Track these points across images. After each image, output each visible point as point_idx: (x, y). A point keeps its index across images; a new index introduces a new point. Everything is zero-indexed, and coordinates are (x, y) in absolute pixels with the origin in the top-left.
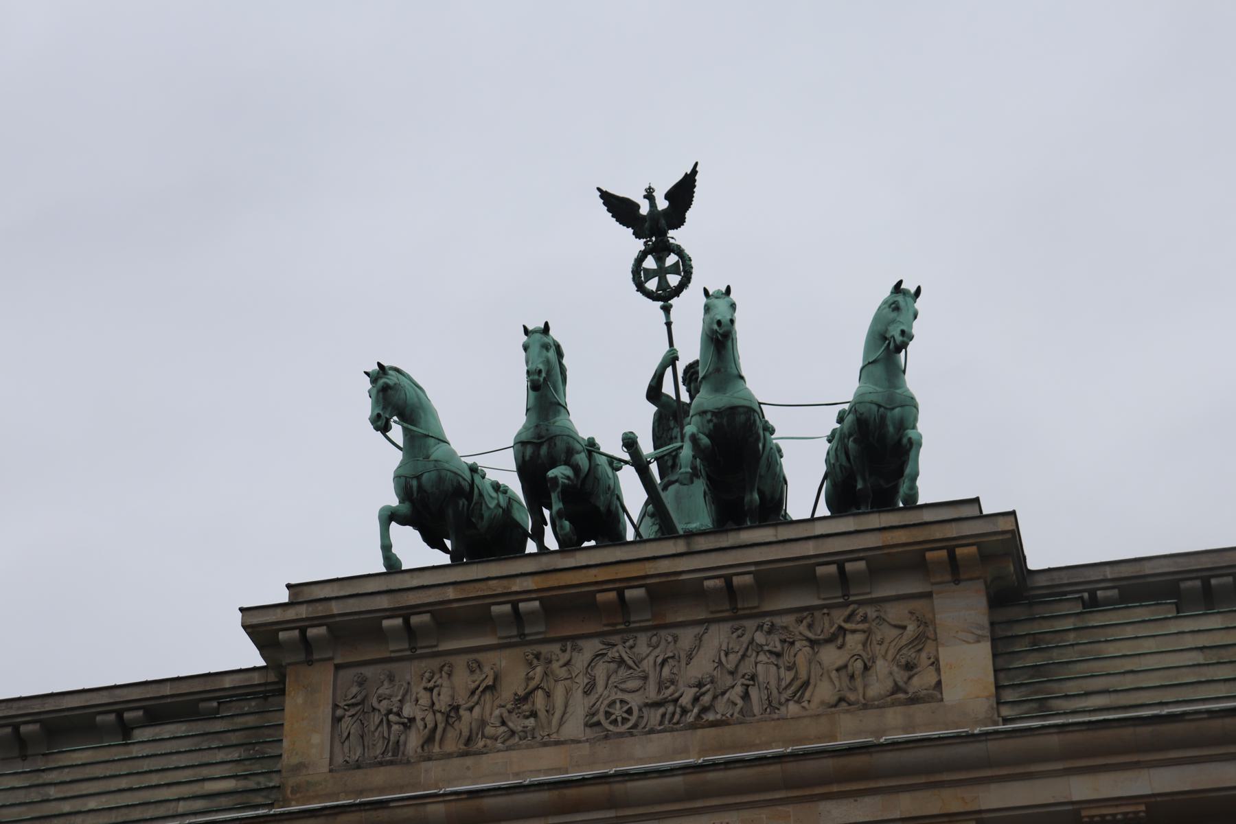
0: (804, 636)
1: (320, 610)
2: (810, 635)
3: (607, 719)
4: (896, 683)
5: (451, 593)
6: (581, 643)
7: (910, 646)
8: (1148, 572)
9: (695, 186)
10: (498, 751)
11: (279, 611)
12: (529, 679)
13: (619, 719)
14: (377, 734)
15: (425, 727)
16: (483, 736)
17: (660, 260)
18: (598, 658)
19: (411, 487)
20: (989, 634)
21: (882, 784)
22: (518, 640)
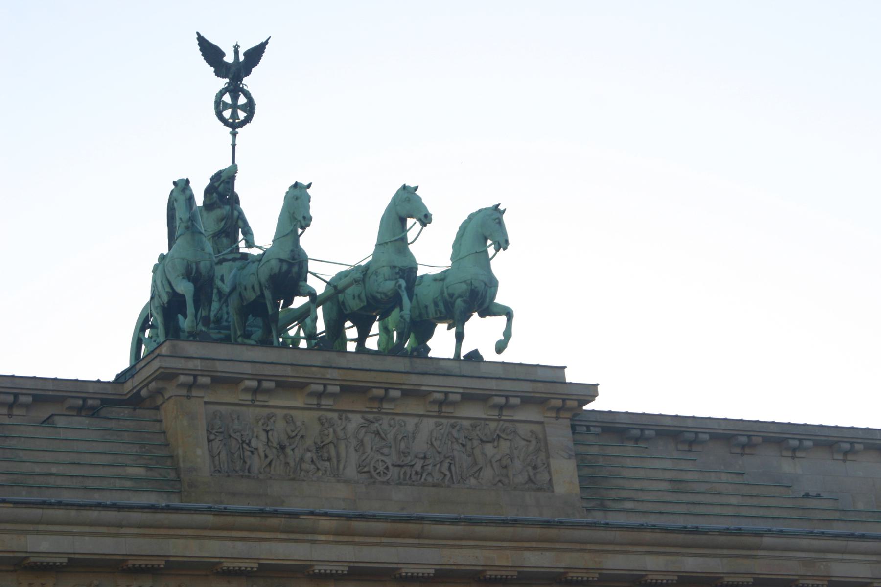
0: (479, 437)
2: (482, 438)
3: (375, 471)
4: (529, 477)
5: (289, 371)
6: (350, 416)
7: (534, 454)
8: (617, 421)
9: (264, 52)
11: (183, 360)
13: (382, 472)
14: (236, 456)
15: (266, 456)
16: (300, 468)
17: (235, 98)
18: (362, 428)
19: (192, 269)
20: (574, 455)
21: (558, 546)
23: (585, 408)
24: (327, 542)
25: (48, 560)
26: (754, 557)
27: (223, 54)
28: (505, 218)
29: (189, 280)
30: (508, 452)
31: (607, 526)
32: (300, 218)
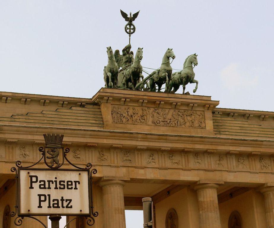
1: (112, 95)
4: (199, 125)
5: (134, 96)
6: (151, 108)
10: (139, 125)
12: (143, 113)
15: (127, 118)
17: (130, 27)
21: (205, 143)
22: (141, 106)
23: (216, 107)
24: (141, 141)
25: (66, 143)
26: (261, 147)
27: (127, 15)
28: (197, 57)
29: (111, 73)
30: (194, 118)
31: (219, 138)
32: (140, 57)
